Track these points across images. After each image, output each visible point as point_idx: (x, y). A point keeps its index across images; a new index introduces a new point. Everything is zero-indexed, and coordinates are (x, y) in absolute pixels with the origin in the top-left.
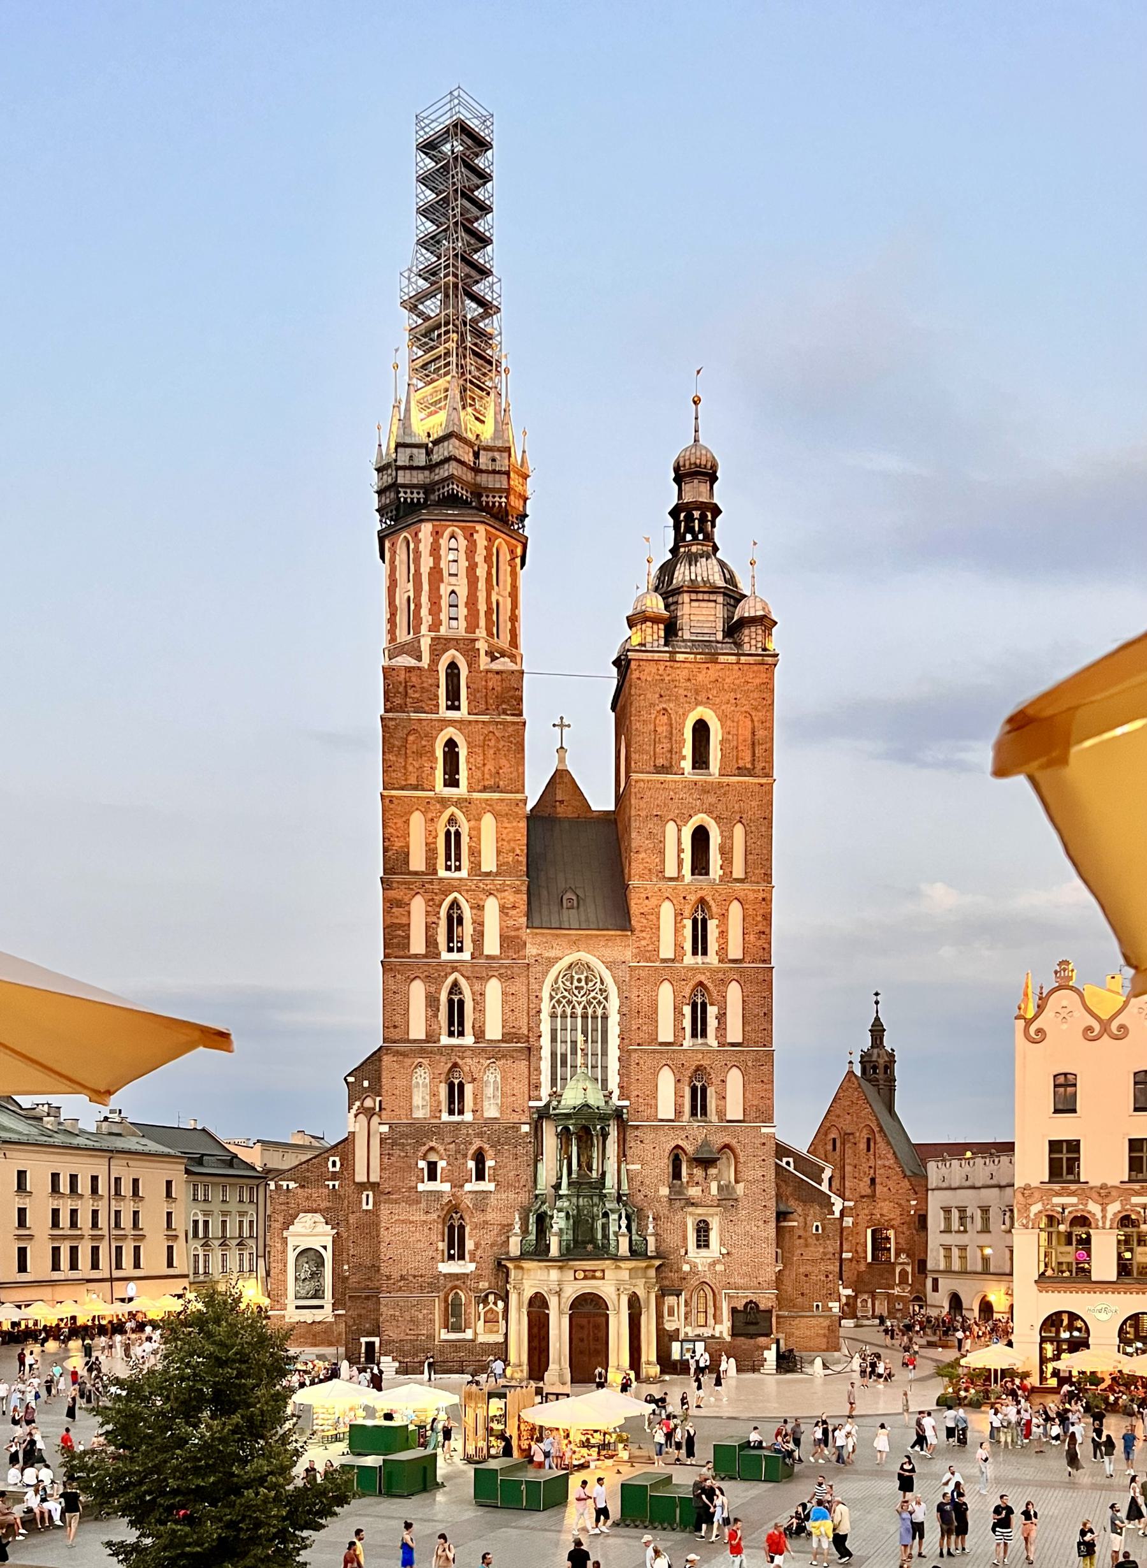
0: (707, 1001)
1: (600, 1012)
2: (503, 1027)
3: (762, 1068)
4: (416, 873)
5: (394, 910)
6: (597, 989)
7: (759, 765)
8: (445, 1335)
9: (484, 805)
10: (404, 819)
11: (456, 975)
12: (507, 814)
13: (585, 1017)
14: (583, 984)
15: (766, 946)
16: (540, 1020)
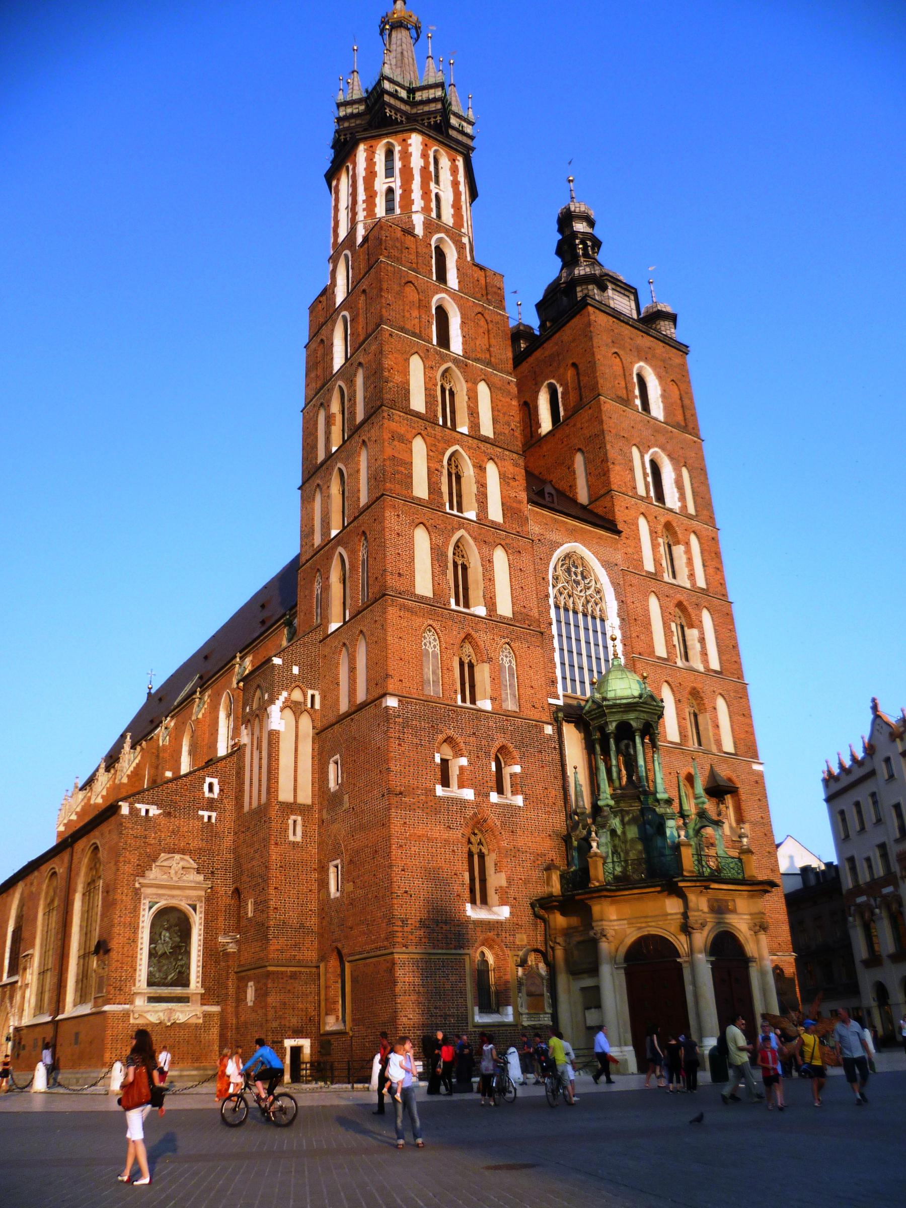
0: (684, 623)
1: (598, 613)
2: (513, 604)
3: (741, 700)
4: (417, 415)
5: (396, 443)
6: (593, 588)
7: (691, 426)
8: (480, 1019)
9: (480, 374)
10: (405, 357)
11: (462, 532)
12: (500, 389)
13: (585, 615)
14: (579, 578)
15: (722, 581)
16: (550, 606)
